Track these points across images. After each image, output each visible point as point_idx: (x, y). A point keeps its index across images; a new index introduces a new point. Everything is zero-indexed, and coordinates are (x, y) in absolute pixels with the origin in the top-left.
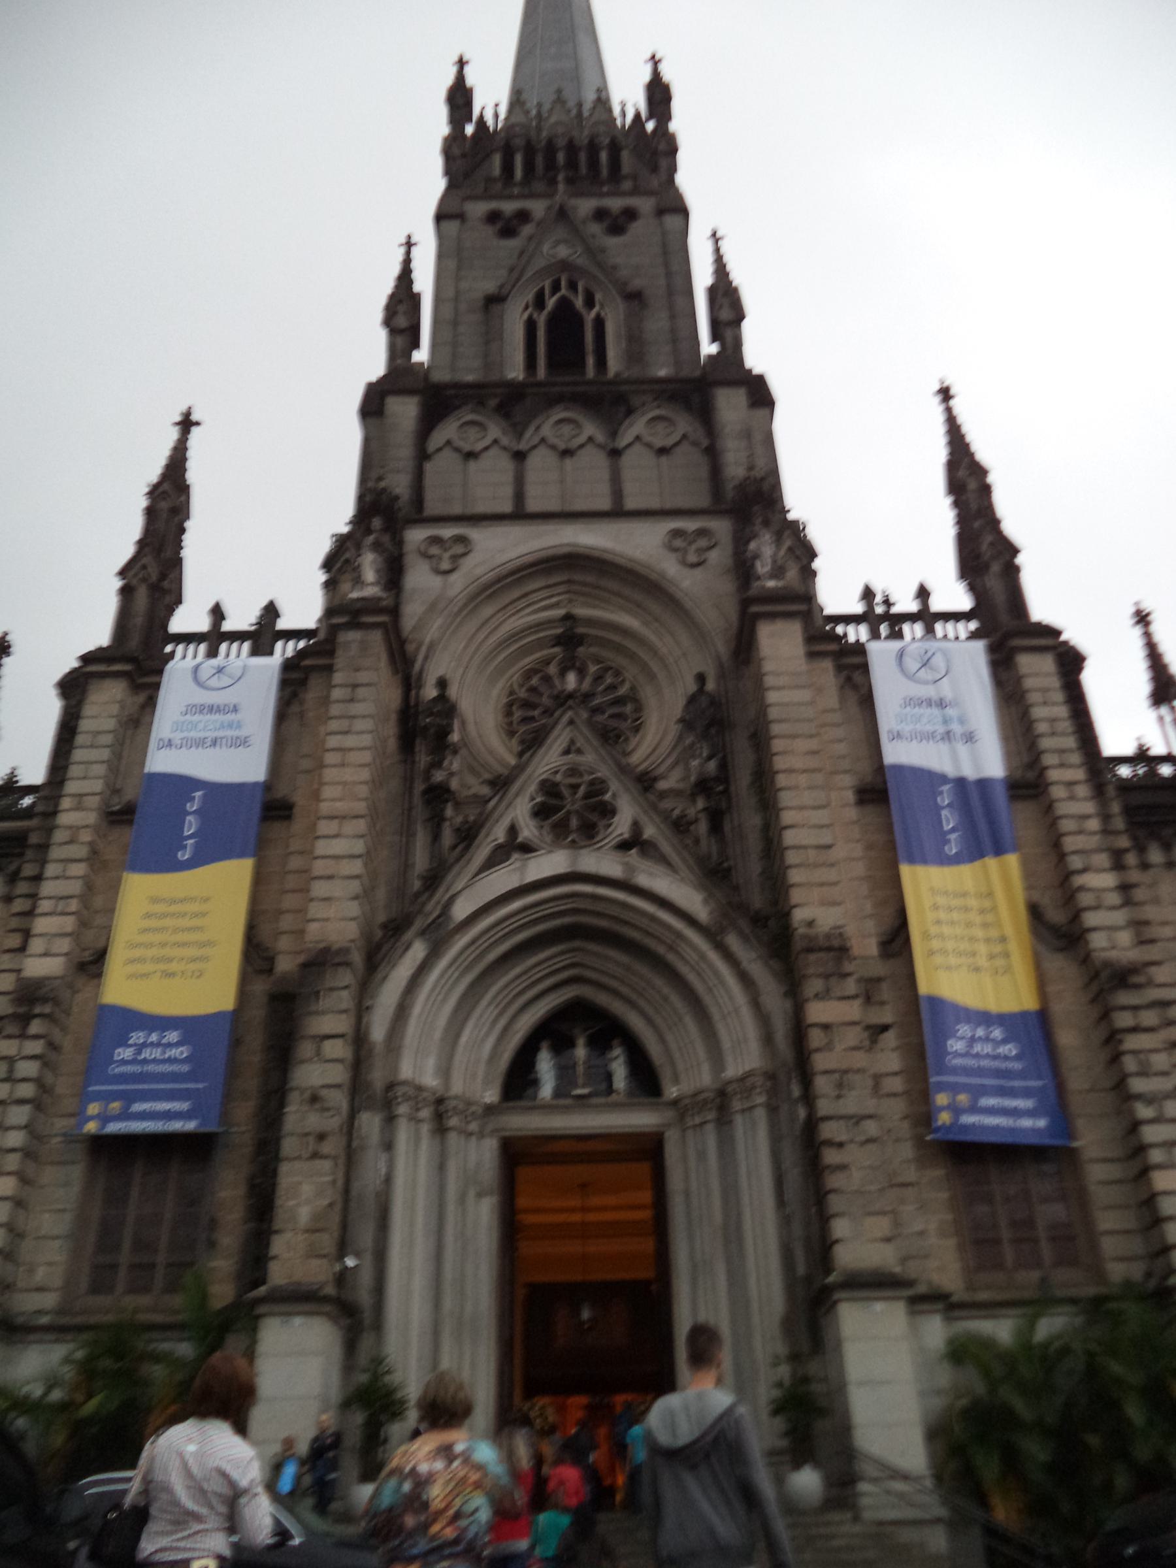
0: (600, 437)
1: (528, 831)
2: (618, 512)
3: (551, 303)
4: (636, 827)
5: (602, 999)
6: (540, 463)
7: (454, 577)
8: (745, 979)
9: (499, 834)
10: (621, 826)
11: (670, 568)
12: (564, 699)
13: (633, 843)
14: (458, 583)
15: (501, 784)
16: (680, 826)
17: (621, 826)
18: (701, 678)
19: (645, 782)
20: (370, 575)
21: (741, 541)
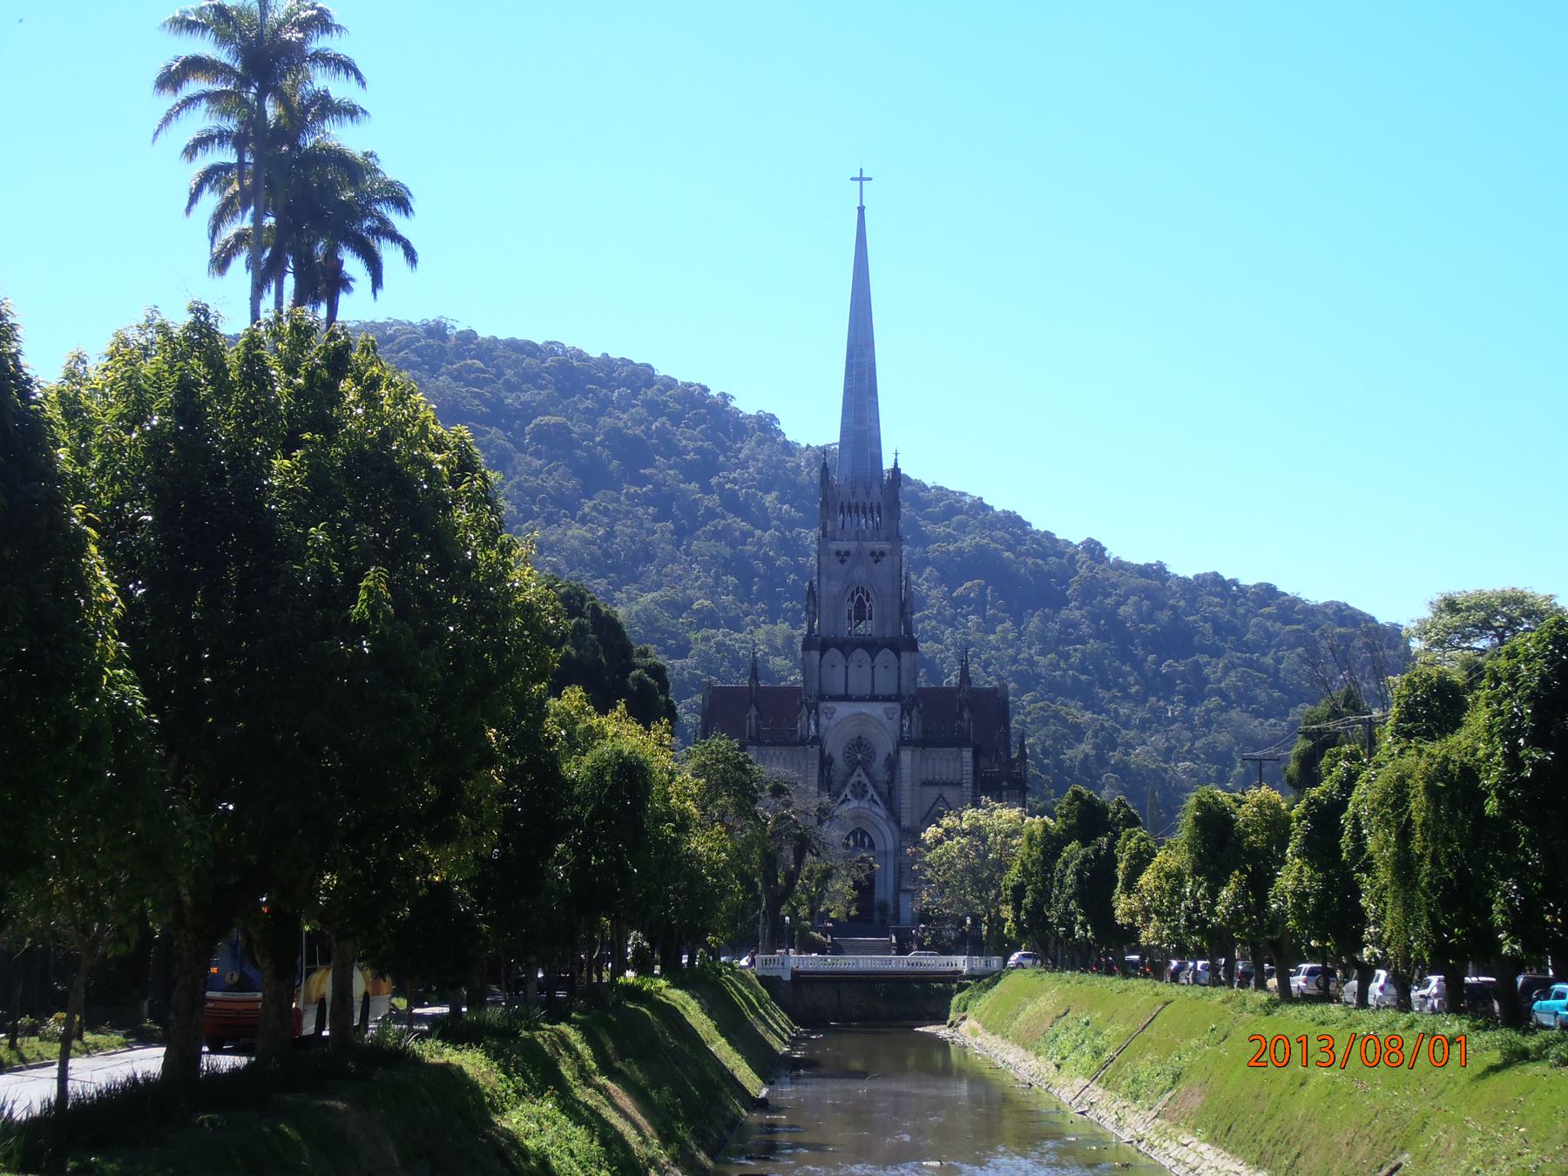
0: (869, 660)
1: (849, 797)
2: (874, 698)
3: (856, 598)
4: (872, 796)
5: (864, 828)
6: (853, 668)
7: (831, 721)
8: (891, 830)
9: (843, 797)
10: (869, 796)
11: (885, 720)
12: (859, 763)
13: (873, 800)
14: (833, 722)
15: (844, 785)
16: (880, 795)
17: (869, 796)
18: (889, 755)
19: (875, 787)
20: (813, 727)
21: (902, 718)
